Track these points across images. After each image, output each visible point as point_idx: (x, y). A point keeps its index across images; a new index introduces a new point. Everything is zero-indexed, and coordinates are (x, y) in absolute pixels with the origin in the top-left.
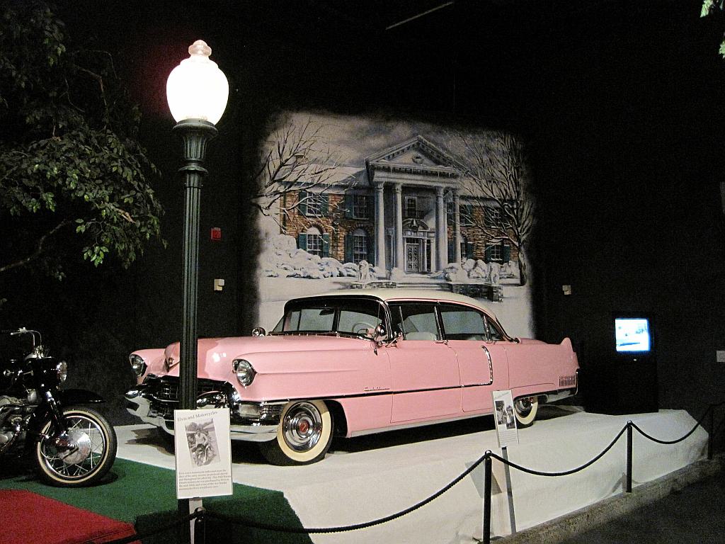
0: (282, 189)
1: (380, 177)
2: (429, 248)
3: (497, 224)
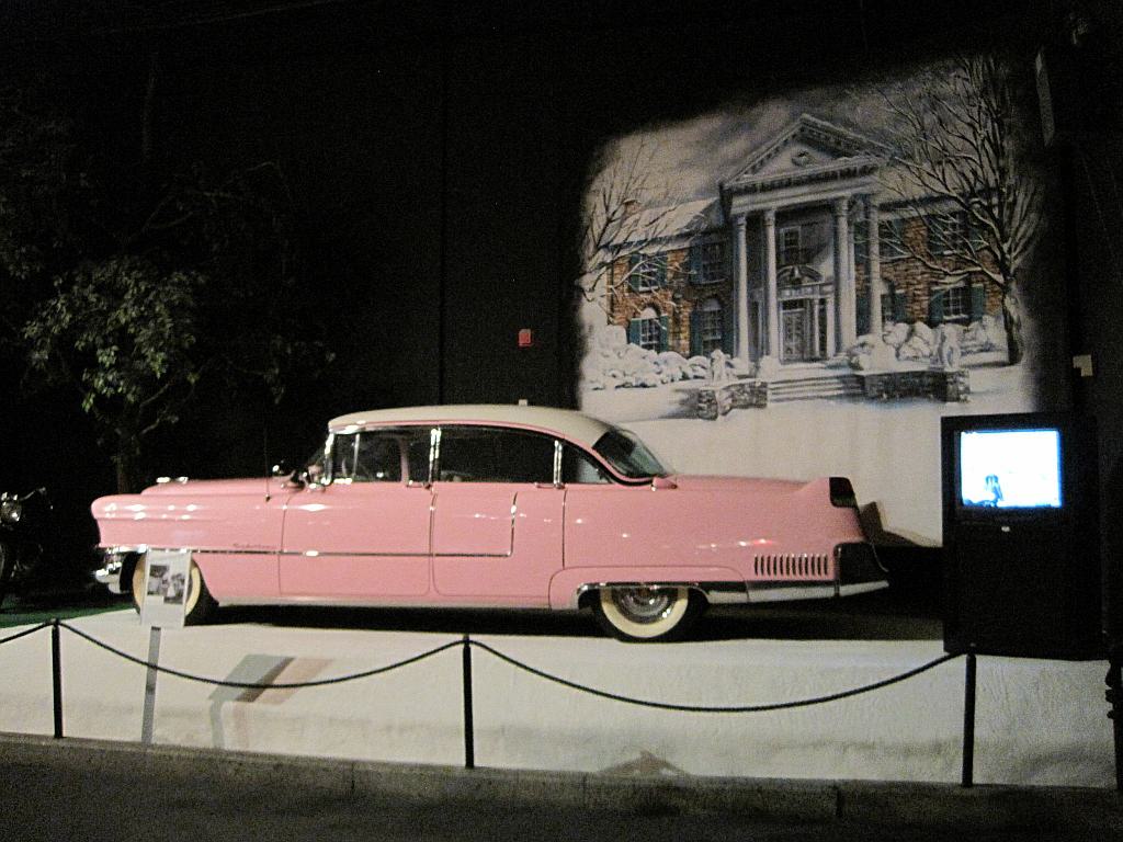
0: (608, 259)
2: (823, 312)
3: (955, 246)
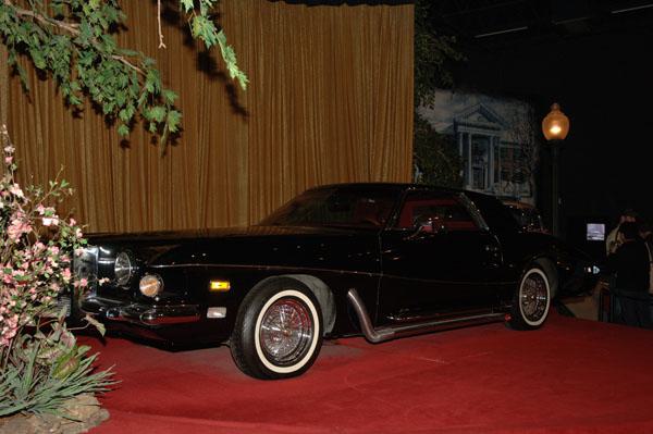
1: (461, 129)
